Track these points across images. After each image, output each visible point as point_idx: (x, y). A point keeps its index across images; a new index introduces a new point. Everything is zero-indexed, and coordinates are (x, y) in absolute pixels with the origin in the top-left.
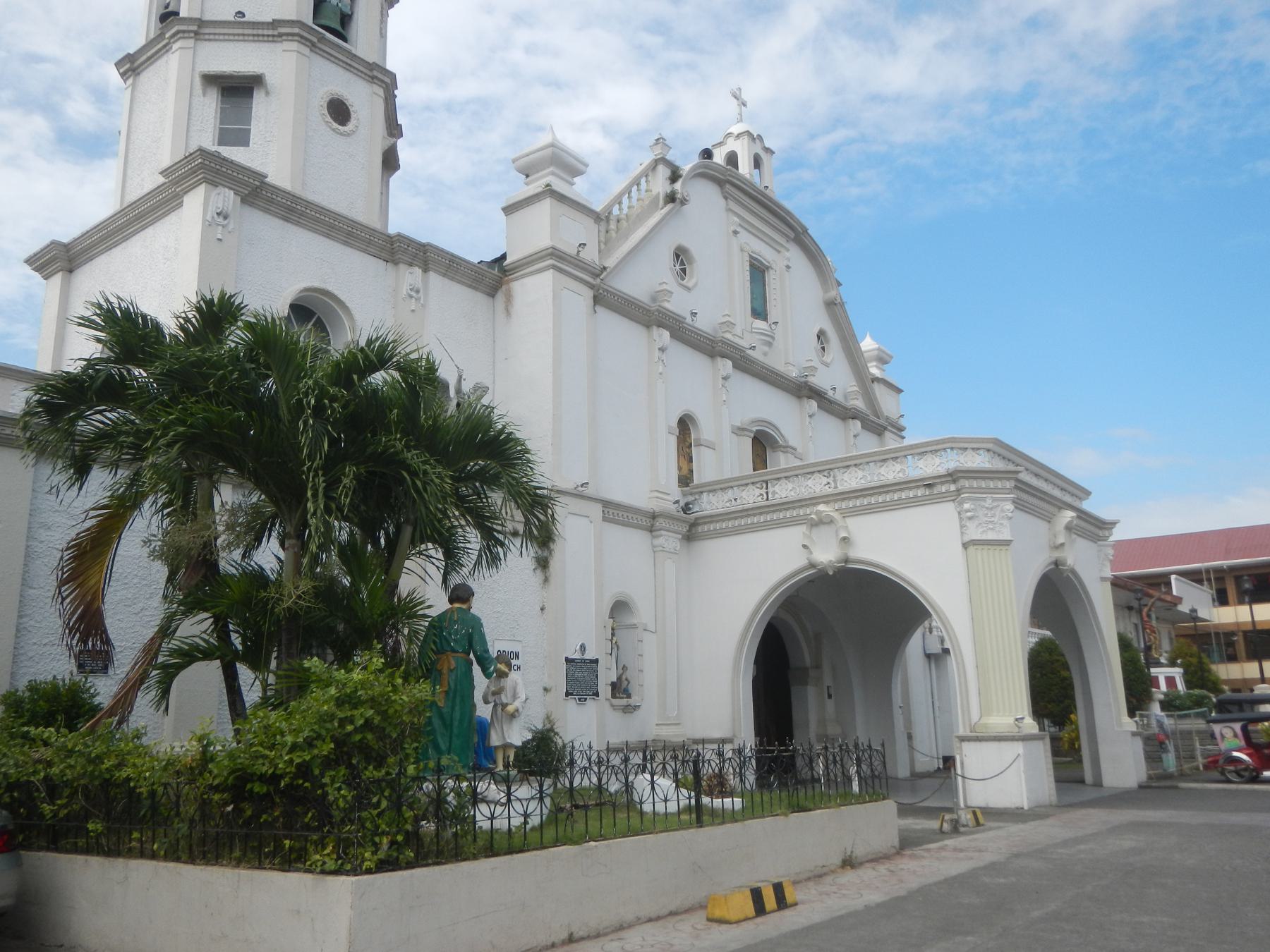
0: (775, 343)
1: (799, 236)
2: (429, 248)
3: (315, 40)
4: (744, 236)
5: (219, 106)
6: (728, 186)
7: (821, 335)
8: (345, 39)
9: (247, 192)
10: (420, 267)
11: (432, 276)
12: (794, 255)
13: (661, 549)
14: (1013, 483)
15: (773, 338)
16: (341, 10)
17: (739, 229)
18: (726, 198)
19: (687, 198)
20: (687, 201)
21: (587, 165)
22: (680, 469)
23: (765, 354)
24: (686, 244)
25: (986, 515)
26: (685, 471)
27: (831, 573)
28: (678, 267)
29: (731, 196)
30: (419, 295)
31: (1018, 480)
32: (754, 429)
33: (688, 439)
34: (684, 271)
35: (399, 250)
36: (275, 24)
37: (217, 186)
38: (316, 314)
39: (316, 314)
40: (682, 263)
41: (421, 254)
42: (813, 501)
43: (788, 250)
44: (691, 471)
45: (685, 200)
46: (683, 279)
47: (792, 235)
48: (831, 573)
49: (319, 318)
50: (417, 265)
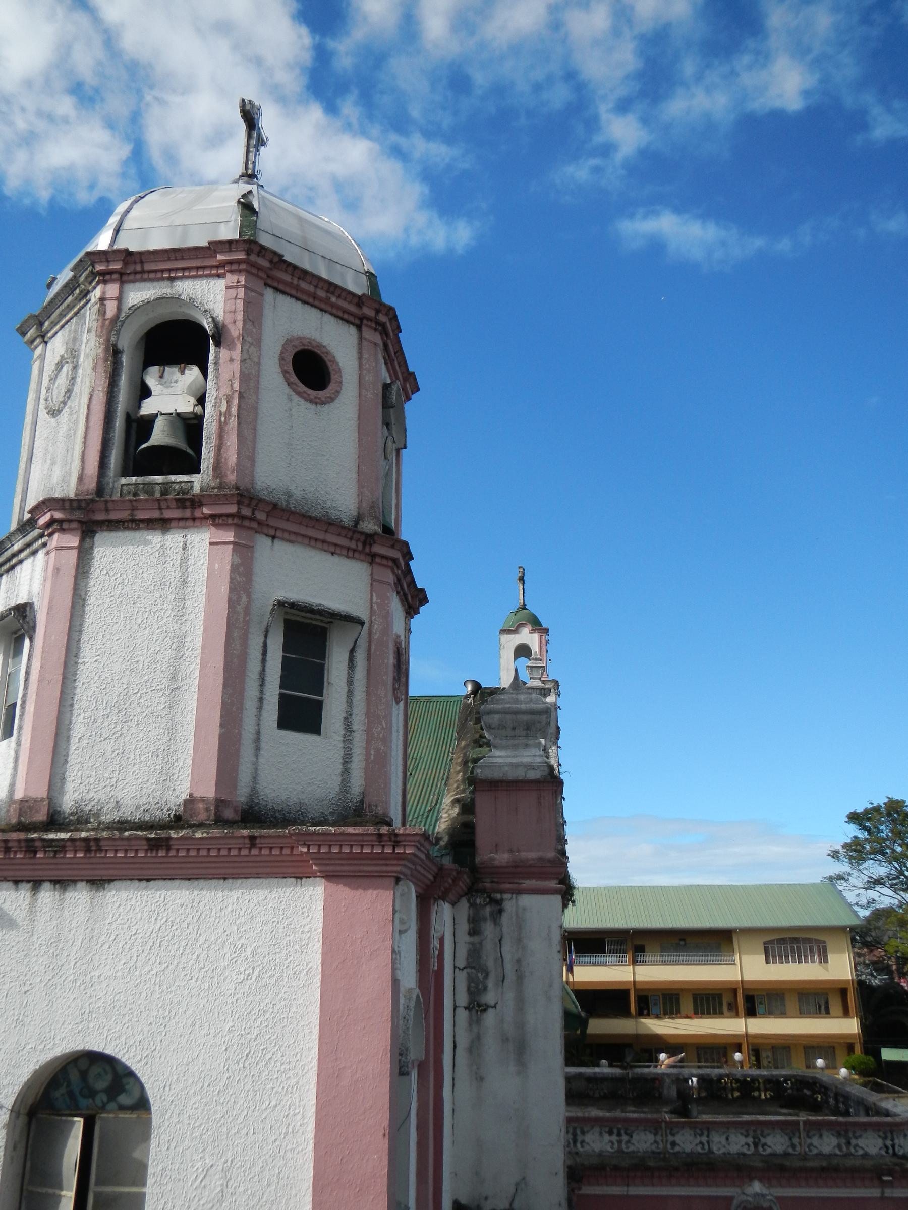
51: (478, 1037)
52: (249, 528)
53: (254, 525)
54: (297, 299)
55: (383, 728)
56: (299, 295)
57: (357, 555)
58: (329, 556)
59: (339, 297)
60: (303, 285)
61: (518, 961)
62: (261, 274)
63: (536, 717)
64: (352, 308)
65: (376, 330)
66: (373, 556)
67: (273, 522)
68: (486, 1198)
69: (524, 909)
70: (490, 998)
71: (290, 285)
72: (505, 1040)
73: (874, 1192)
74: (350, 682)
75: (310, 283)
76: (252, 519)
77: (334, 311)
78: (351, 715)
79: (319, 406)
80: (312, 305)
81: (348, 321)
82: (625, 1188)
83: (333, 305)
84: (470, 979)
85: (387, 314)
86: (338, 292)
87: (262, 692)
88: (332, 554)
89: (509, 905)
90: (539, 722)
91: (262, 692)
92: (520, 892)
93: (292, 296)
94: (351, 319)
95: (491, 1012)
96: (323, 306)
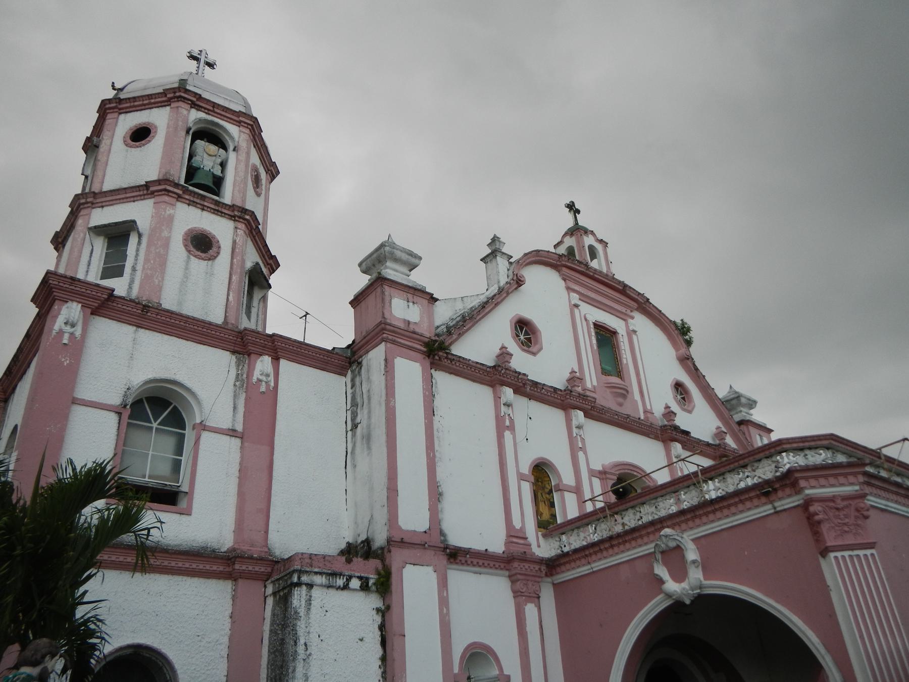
0: (629, 396)
1: (643, 306)
2: (275, 337)
3: (180, 192)
4: (585, 308)
5: (105, 251)
6: (564, 269)
7: (679, 387)
8: (218, 195)
9: (96, 305)
10: (269, 355)
11: (283, 363)
12: (640, 322)
13: (519, 594)
14: (861, 479)
15: (627, 392)
16: (213, 174)
17: (580, 303)
18: (565, 280)
19: (522, 279)
20: (522, 281)
21: (420, 258)
22: (538, 513)
23: (621, 405)
24: (527, 315)
25: (838, 517)
26: (546, 516)
27: (688, 602)
28: (522, 337)
29: (568, 277)
30: (269, 379)
31: (866, 474)
32: (617, 473)
33: (547, 486)
34: (529, 340)
35: (248, 343)
36: (147, 185)
37: (67, 302)
38: (171, 404)
39: (171, 404)
40: (526, 333)
41: (270, 344)
42: (657, 524)
43: (633, 318)
44: (554, 516)
45: (520, 280)
46: (529, 347)
47: (635, 305)
48: (688, 602)
49: (175, 407)
50: (267, 354)
51: (355, 443)
52: (88, 207)
53: (89, 205)
54: (137, 111)
55: (151, 264)
56: (137, 108)
57: (146, 197)
58: (132, 204)
59: (156, 98)
60: (136, 103)
61: (369, 391)
62: (115, 110)
63: (378, 252)
64: (164, 99)
65: (178, 101)
66: (153, 193)
67: (98, 200)
68: (359, 535)
69: (370, 359)
70: (358, 420)
71: (130, 107)
72: (363, 438)
73: (767, 509)
74: (138, 250)
75: (140, 101)
76: (87, 203)
77: (156, 105)
78: (136, 264)
79: (142, 147)
80: (145, 109)
81: (165, 106)
82: (589, 567)
83: (154, 103)
84: (352, 413)
85: (180, 91)
86: (154, 97)
87: (88, 268)
88: (134, 201)
89: (364, 363)
90: (381, 254)
91: (88, 268)
92: (367, 352)
93: (134, 111)
94: (166, 103)
95: (359, 425)
96: (150, 106)
